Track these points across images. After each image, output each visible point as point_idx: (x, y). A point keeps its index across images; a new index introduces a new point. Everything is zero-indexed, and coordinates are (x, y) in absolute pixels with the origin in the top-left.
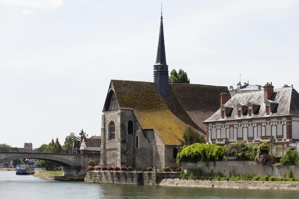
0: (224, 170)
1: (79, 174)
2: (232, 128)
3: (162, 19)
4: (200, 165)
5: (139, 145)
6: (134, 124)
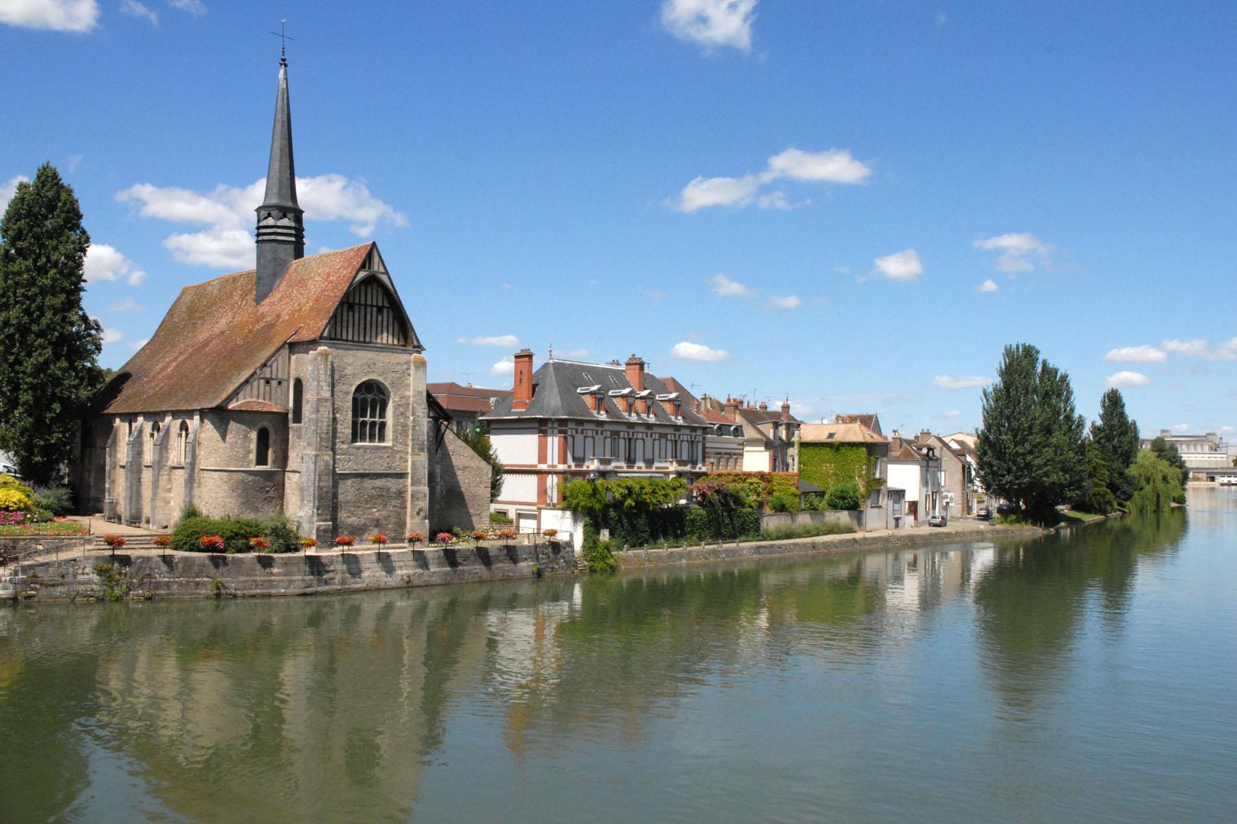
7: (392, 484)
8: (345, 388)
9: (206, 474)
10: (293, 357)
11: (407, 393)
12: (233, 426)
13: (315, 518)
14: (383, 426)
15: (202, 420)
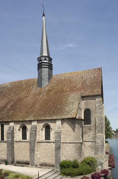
9: (65, 145)
10: (84, 102)
12: (77, 125)
15: (62, 123)
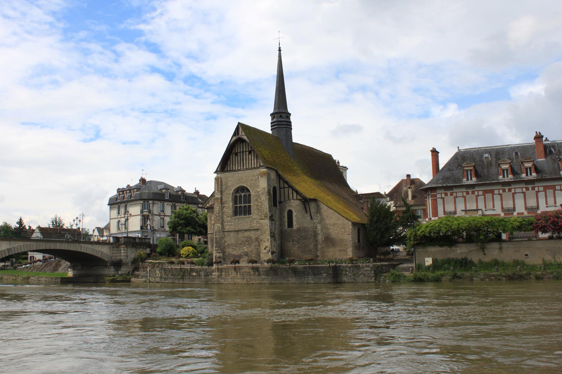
0: (526, 255)
1: (120, 272)
2: (489, 196)
3: (280, 50)
4: (460, 251)
5: (295, 223)
6: (278, 191)
7: (253, 234)
8: (228, 192)
11: (258, 190)
13: (215, 252)
14: (250, 206)
